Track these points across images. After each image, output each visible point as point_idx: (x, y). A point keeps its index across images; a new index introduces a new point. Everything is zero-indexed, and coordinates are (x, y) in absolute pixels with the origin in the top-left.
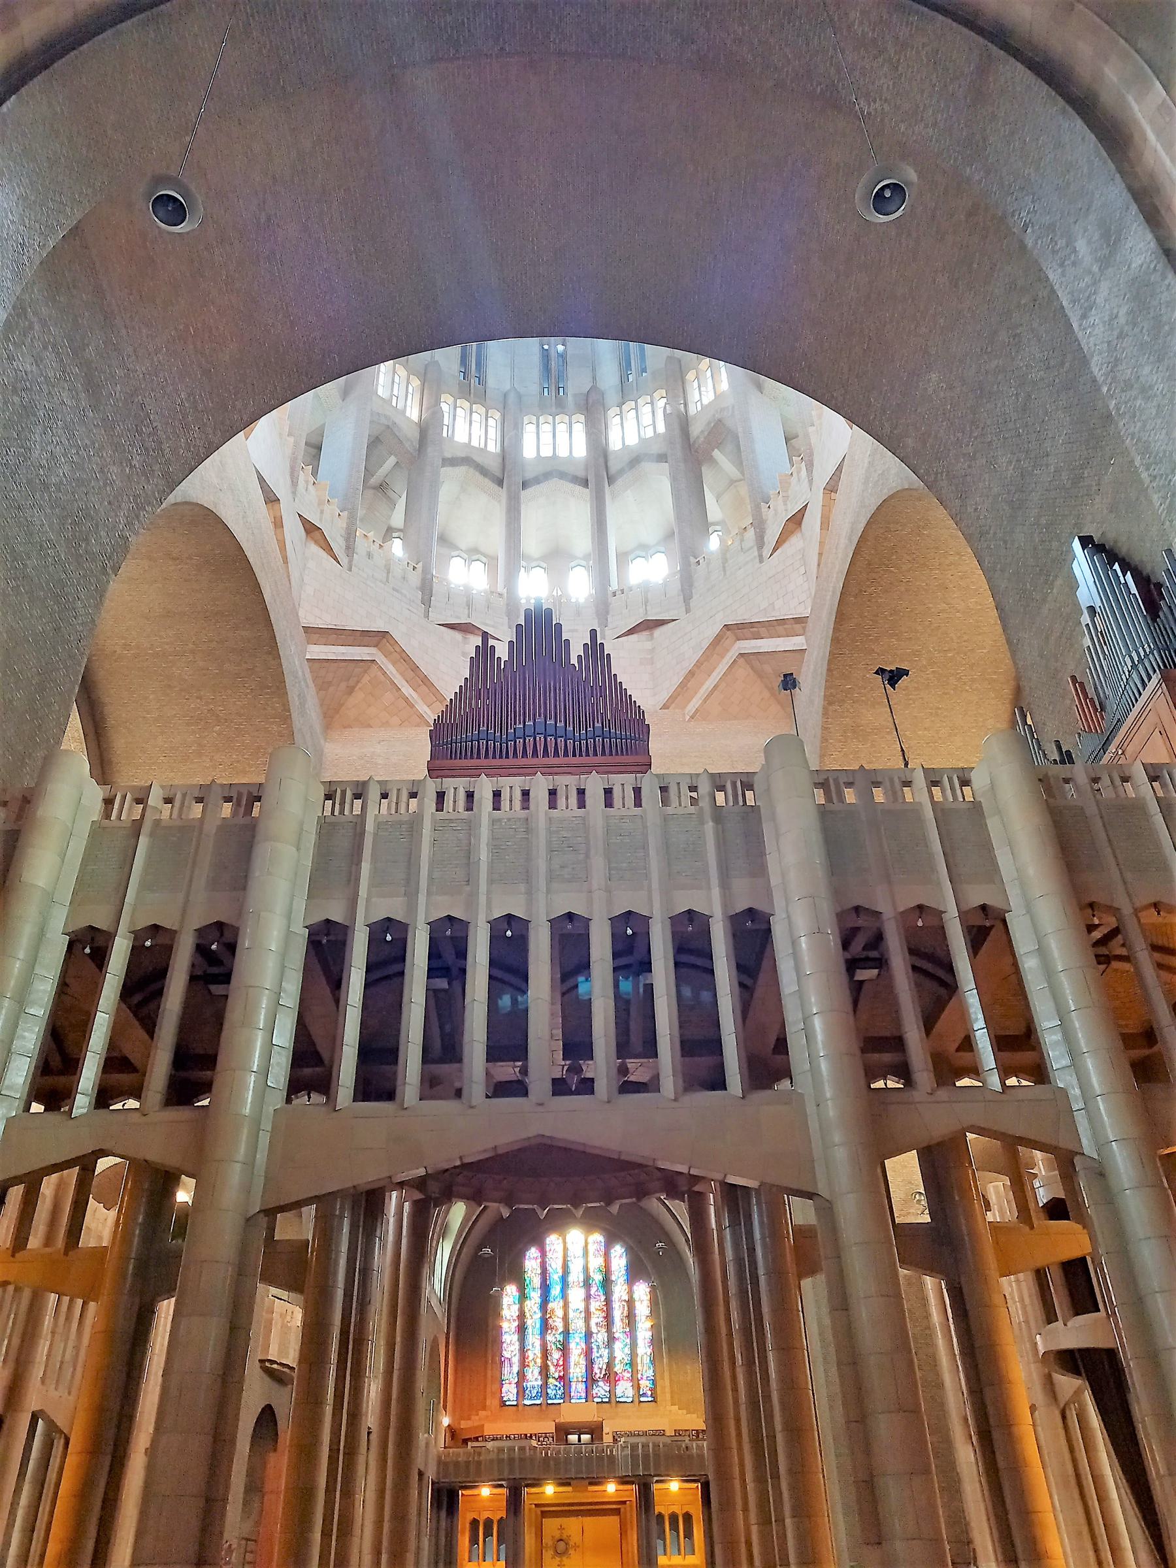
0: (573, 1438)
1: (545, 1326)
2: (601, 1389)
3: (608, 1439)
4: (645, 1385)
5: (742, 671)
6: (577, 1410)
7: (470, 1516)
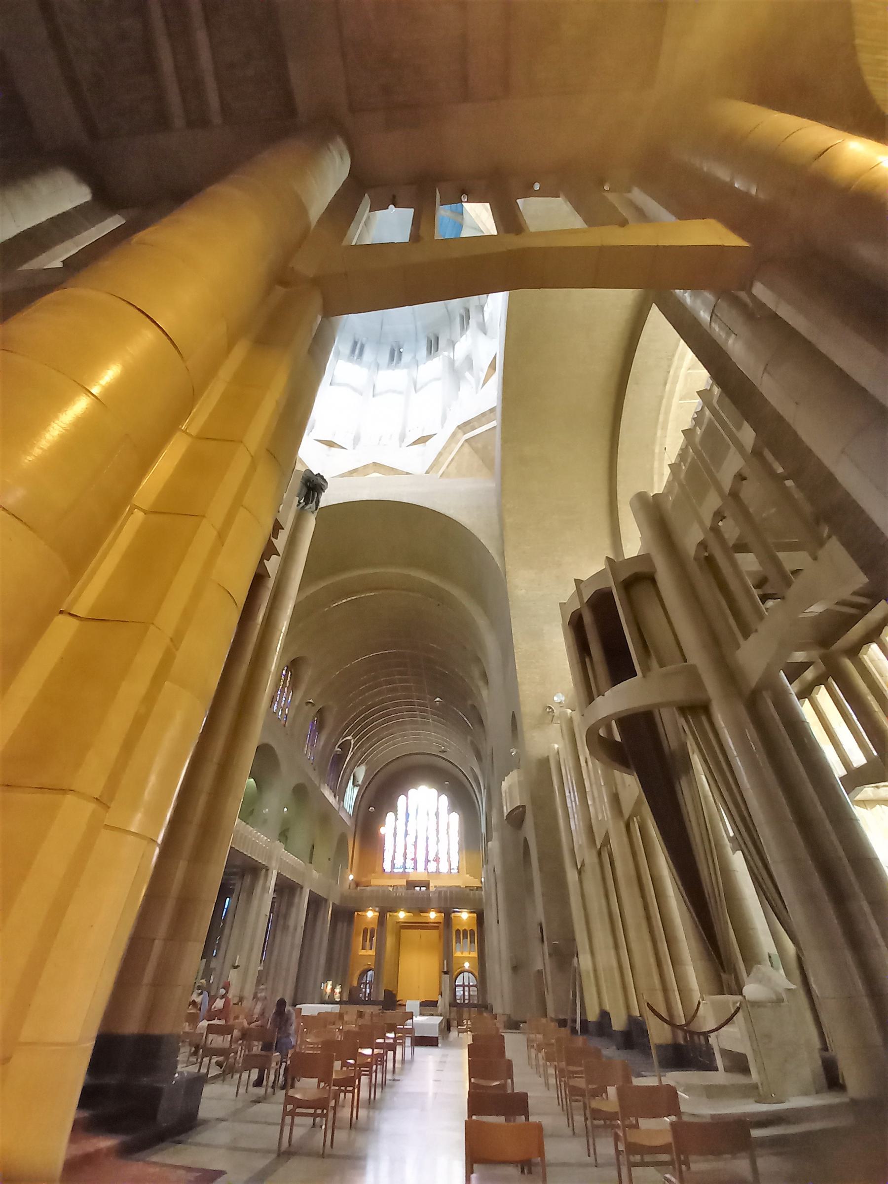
0: (418, 889)
1: (406, 834)
2: (432, 867)
3: (432, 889)
4: (455, 865)
5: (467, 449)
6: (420, 874)
7: (363, 927)
